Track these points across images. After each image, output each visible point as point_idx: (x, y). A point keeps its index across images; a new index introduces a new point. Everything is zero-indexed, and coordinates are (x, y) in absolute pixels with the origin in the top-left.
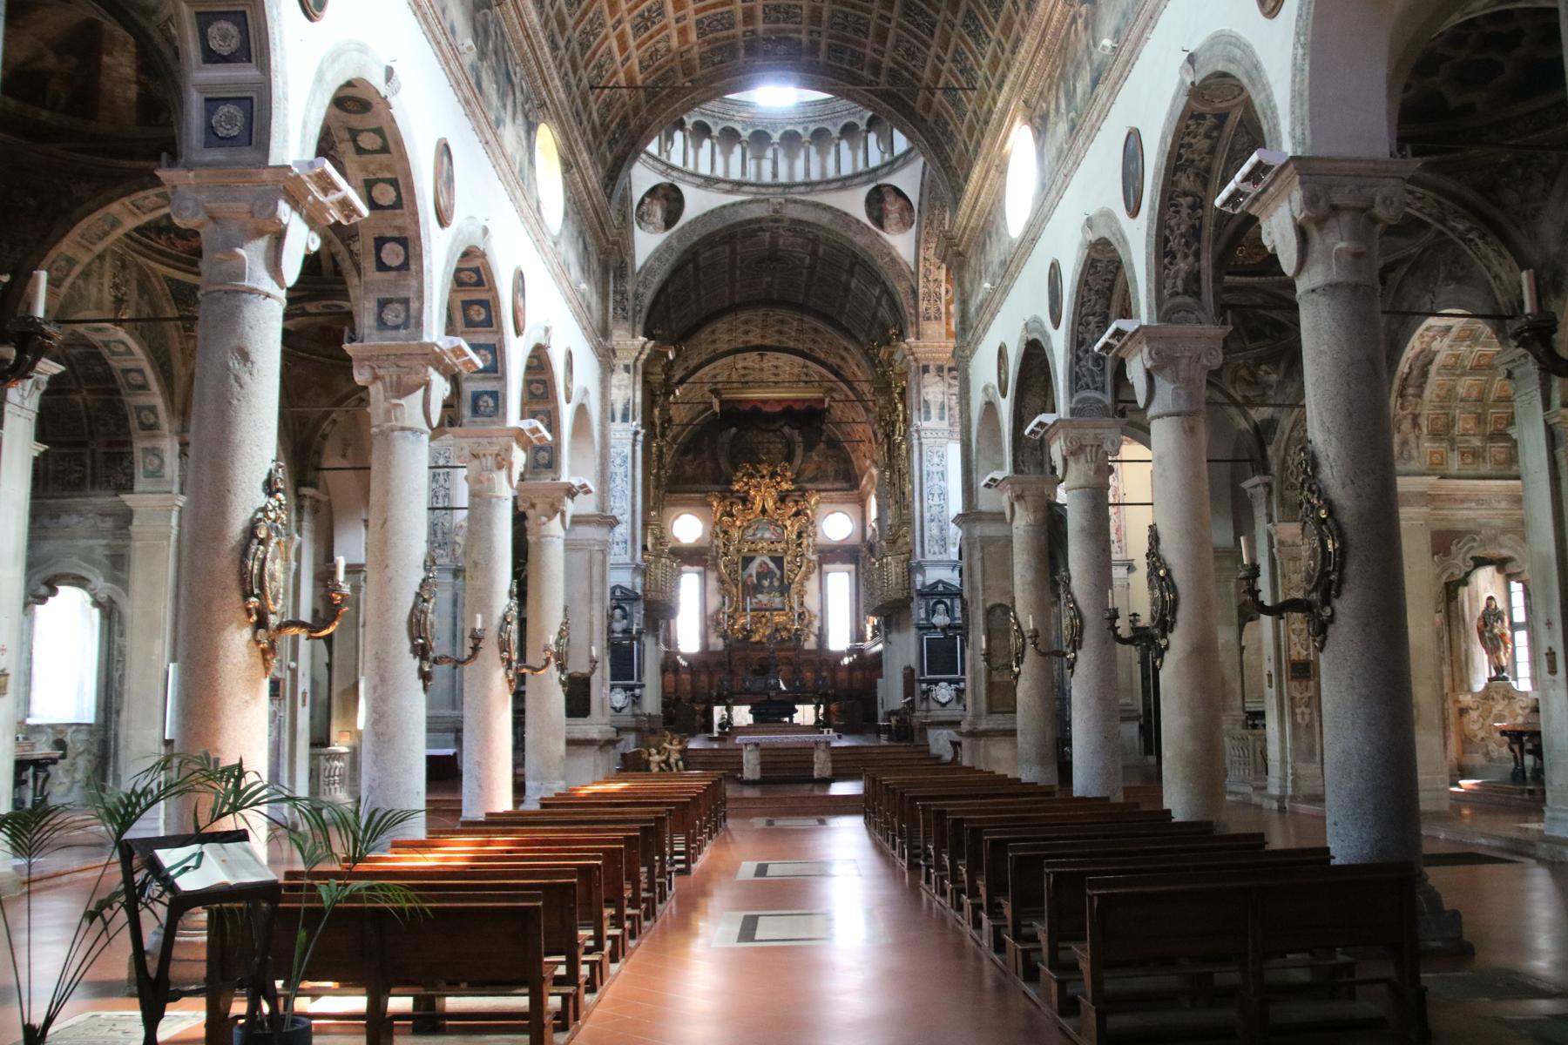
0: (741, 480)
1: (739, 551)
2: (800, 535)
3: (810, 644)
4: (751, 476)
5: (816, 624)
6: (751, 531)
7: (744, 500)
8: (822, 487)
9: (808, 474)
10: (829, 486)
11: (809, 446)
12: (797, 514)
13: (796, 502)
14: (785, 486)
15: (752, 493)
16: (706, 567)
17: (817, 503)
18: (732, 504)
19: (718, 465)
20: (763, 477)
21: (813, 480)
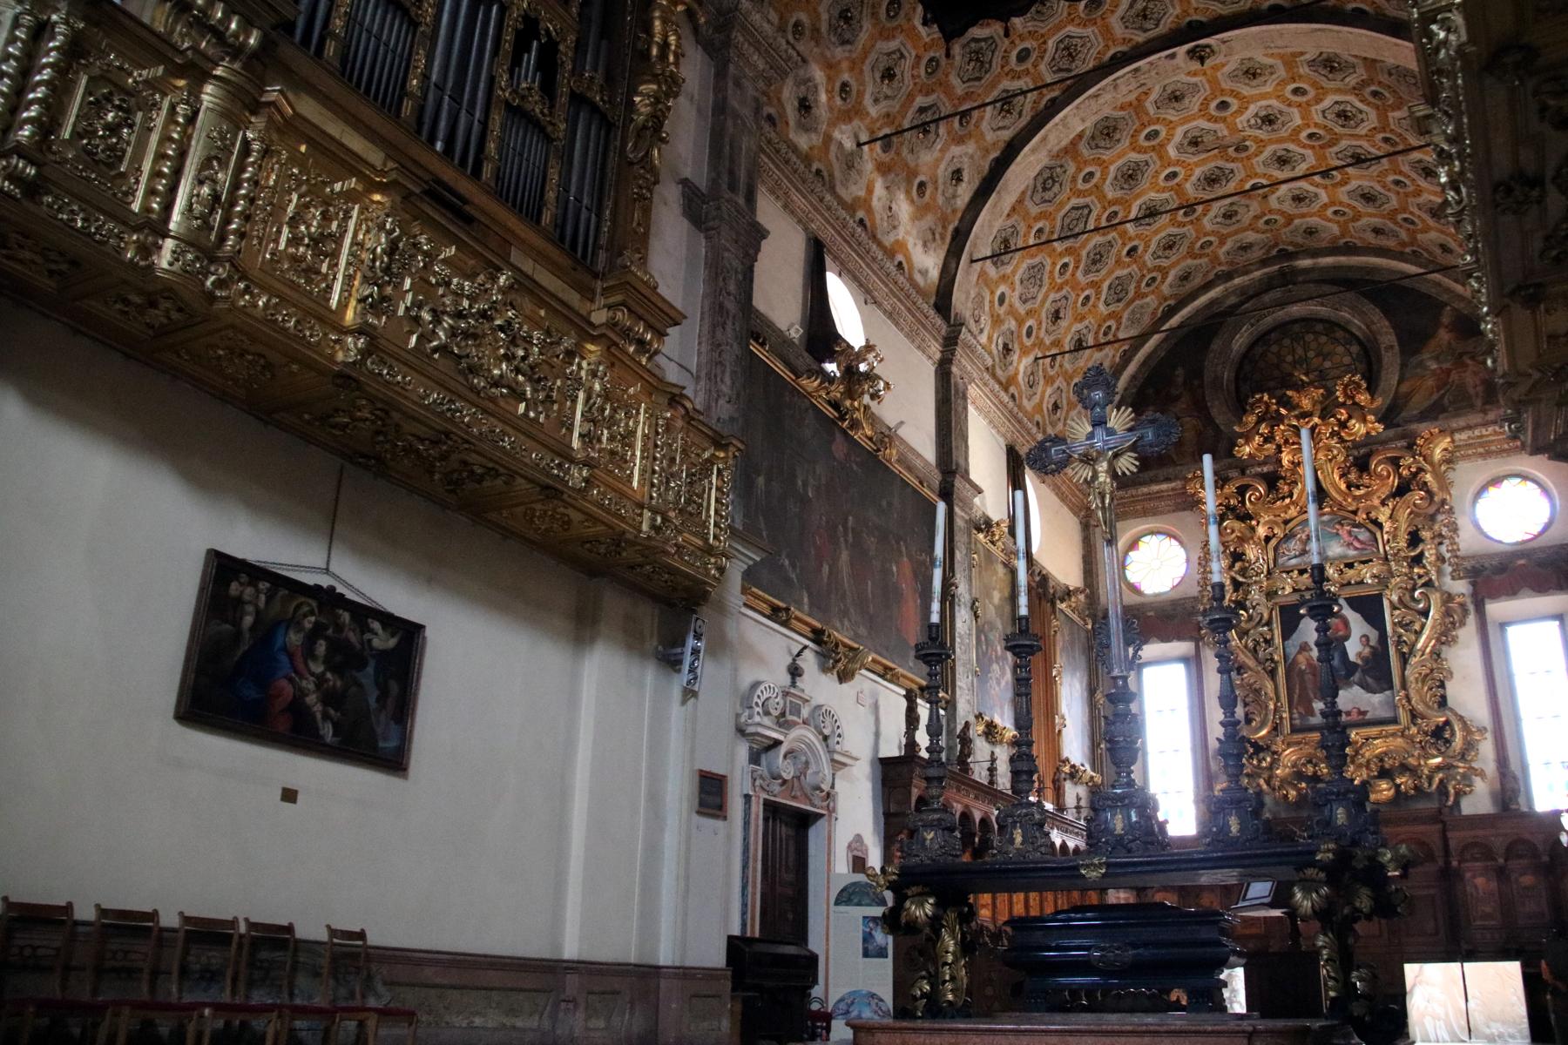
0: (1255, 430)
1: (1270, 594)
2: (1414, 539)
3: (1478, 801)
4: (1279, 419)
5: (1487, 748)
6: (1294, 546)
7: (1272, 480)
8: (1462, 422)
9: (1419, 402)
10: (1476, 418)
11: (1412, 342)
12: (1402, 490)
13: (1395, 462)
14: (1358, 428)
15: (1286, 458)
16: (1197, 640)
17: (1449, 461)
18: (1241, 491)
19: (1209, 420)
20: (1306, 415)
21: (1433, 412)
